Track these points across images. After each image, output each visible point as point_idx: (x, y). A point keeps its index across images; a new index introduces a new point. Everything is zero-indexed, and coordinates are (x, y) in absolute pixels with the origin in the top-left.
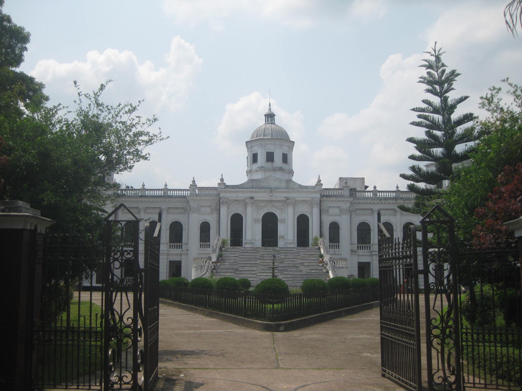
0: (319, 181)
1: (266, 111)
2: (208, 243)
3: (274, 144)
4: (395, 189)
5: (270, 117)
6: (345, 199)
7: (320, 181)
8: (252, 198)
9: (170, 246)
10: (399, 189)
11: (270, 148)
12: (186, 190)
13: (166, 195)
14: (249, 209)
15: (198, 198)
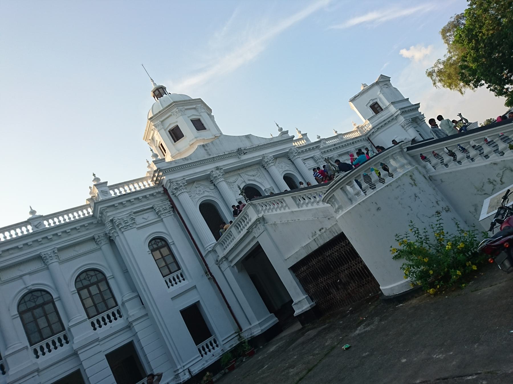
0: (281, 129)
1: (153, 87)
2: (178, 273)
3: (195, 108)
4: (336, 134)
5: (159, 92)
6: (314, 146)
7: (281, 129)
8: (217, 168)
9: (93, 324)
10: (339, 133)
11: (193, 114)
12: (81, 208)
13: (41, 228)
14: (223, 185)
15: (123, 200)
